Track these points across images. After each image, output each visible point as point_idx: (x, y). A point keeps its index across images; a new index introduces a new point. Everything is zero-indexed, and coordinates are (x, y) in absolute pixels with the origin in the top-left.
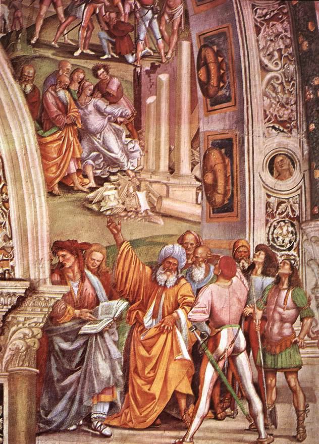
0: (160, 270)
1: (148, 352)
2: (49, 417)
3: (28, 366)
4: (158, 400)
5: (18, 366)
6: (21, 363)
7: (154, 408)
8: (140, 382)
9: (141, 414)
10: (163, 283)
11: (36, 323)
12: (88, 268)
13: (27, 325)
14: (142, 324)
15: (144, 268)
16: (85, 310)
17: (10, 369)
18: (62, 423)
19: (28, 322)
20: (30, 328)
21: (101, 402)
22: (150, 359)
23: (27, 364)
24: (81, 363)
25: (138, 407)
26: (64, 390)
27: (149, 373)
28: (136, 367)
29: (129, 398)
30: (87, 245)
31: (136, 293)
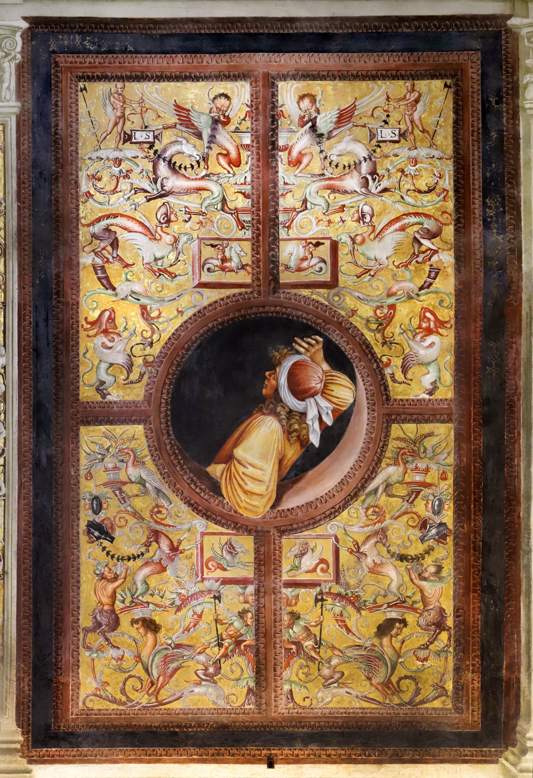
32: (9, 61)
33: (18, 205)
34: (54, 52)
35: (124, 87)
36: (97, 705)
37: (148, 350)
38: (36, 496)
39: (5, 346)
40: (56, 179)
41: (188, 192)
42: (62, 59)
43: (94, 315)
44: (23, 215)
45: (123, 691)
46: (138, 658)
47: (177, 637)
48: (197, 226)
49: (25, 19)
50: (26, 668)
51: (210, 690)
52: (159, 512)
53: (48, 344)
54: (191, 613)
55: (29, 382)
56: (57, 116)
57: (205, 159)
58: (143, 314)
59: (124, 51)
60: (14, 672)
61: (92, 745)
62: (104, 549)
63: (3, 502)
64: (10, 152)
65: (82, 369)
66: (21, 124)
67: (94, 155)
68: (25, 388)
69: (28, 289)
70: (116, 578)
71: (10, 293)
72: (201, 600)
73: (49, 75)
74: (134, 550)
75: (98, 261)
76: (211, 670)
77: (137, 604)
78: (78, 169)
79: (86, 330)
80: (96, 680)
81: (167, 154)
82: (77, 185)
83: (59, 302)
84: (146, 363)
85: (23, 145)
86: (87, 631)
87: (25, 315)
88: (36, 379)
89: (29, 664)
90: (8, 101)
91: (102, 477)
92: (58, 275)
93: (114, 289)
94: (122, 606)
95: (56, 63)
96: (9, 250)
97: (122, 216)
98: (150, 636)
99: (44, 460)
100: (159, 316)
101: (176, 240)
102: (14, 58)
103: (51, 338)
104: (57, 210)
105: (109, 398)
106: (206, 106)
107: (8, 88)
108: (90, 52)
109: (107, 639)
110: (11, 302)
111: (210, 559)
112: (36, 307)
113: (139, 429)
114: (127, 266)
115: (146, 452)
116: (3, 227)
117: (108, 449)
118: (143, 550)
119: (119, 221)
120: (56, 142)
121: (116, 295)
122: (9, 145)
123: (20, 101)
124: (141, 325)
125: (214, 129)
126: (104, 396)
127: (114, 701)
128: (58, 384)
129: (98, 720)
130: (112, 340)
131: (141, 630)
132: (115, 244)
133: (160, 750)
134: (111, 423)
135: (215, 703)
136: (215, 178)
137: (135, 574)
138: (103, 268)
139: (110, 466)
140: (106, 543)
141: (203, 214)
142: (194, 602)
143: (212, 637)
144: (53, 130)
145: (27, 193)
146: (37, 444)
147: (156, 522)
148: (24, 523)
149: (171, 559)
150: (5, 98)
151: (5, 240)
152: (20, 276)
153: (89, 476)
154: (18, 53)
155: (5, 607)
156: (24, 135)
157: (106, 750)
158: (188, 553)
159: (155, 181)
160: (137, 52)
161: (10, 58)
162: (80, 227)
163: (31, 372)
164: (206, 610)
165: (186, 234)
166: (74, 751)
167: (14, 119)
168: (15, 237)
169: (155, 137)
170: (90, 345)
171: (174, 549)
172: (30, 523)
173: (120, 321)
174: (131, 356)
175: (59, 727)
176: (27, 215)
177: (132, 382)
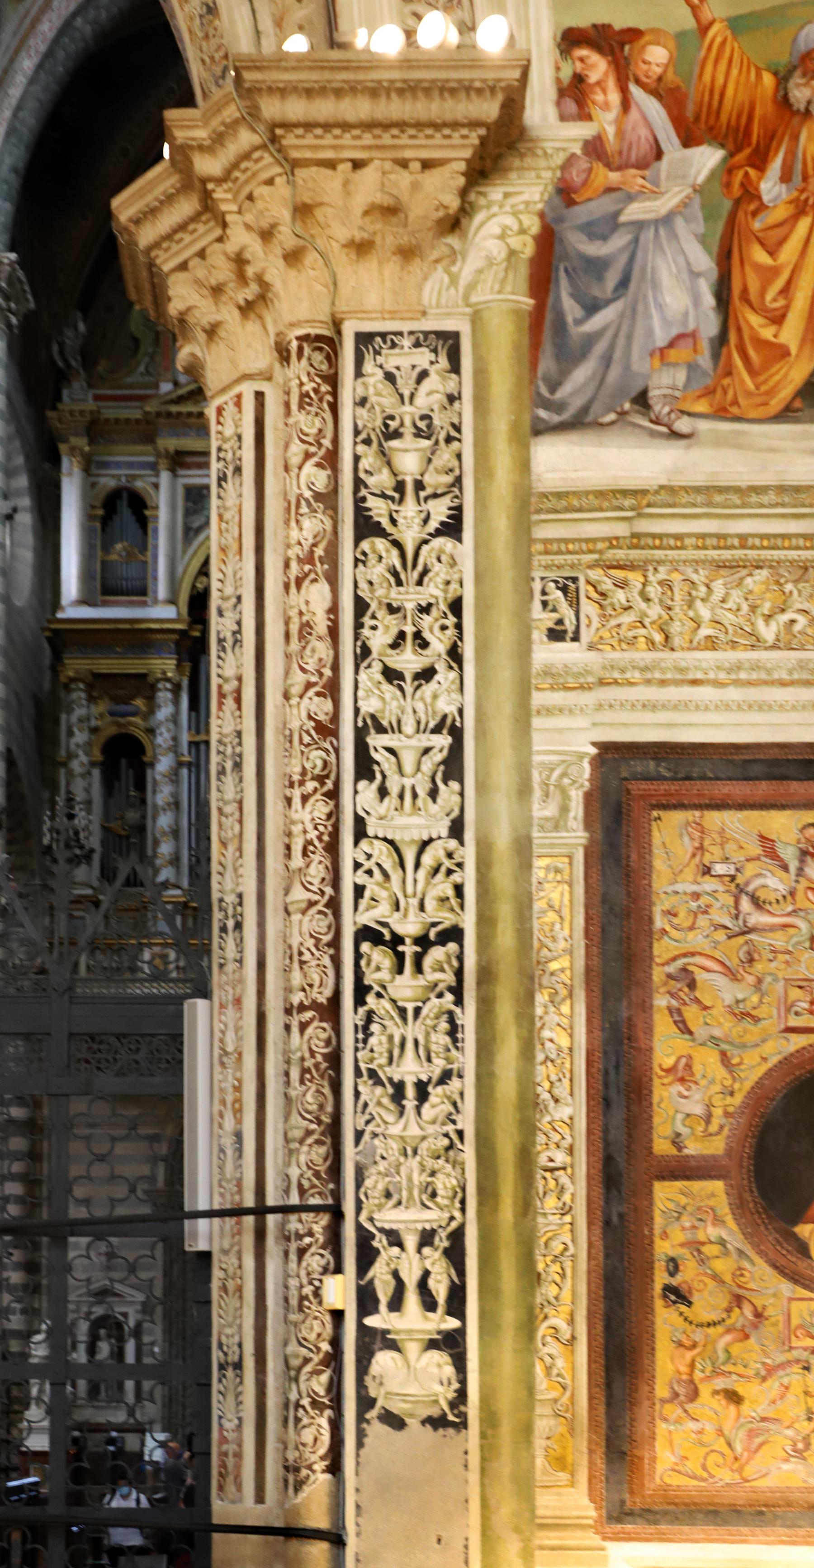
0: (797, 79)
1: (772, 254)
2: (559, 395)
3: (513, 293)
4: (797, 356)
5: (492, 293)
6: (497, 287)
7: (786, 374)
8: (755, 320)
9: (757, 388)
10: (802, 107)
11: (527, 203)
12: (638, 82)
13: (508, 208)
14: (759, 198)
15: (759, 76)
16: (632, 171)
17: (474, 299)
18: (585, 409)
19: (512, 201)
20: (515, 214)
21: (669, 364)
22: (775, 271)
23: (509, 288)
24: (624, 283)
25: (752, 372)
26: (590, 340)
27: (775, 300)
28: (745, 290)
29: (729, 356)
30: (634, 34)
31: (742, 130)
34: (626, 779)
35: (701, 817)
36: (675, 1480)
37: (729, 1100)
38: (607, 1256)
40: (628, 915)
41: (772, 928)
42: (636, 787)
43: (669, 1062)
45: (704, 1468)
46: (720, 1432)
47: (762, 1409)
48: (783, 966)
49: (594, 744)
51: (800, 1467)
52: (742, 1275)
54: (777, 1384)
55: (598, 1133)
57: (792, 893)
58: (722, 1061)
59: (703, 778)
61: (671, 1523)
62: (681, 1314)
65: (656, 1120)
67: (670, 889)
69: (597, 1033)
70: (694, 1346)
71: (576, 1038)
72: (788, 1370)
73: (619, 805)
74: (713, 1317)
75: (674, 1003)
76: (800, 1446)
77: (718, 1374)
78: (651, 904)
79: (660, 1077)
80: (673, 1453)
81: (750, 888)
82: (651, 921)
84: (727, 1114)
86: (663, 1401)
88: (606, 1131)
91: (678, 1236)
92: (629, 1019)
93: (691, 1033)
94: (701, 1375)
95: (628, 791)
97: (700, 954)
98: (732, 1408)
100: (739, 1064)
101: (760, 981)
102: (582, 786)
105: (686, 1151)
106: (793, 835)
107: (575, 818)
108: (665, 779)
109: (686, 1411)
111: (800, 1326)
112: (605, 1053)
113: (718, 1186)
114: (706, 1008)
115: (727, 1210)
117: (684, 1208)
118: (724, 1315)
119: (698, 960)
120: (628, 875)
121: (693, 1040)
124: (721, 1072)
125: (802, 861)
126: (680, 1149)
127: (694, 1477)
128: (630, 1135)
129: (676, 1497)
130: (688, 1089)
131: (724, 1402)
132: (692, 985)
133: (745, 1530)
134: (687, 1178)
135: (805, 1481)
136: (801, 914)
137: (715, 1341)
138: (679, 1012)
139: (687, 1224)
140: (683, 1308)
141: (789, 953)
142: (781, 1373)
143: (801, 1411)
145: (595, 930)
146: (607, 1201)
147: (739, 1286)
149: (755, 1326)
153: (665, 1235)
157: (686, 1528)
158: (773, 1319)
159: (737, 917)
160: (718, 779)
162: (654, 966)
164: (794, 1382)
165: (770, 974)
166: (652, 1529)
169: (737, 870)
170: (665, 1094)
171: (758, 1315)
173: (697, 1068)
174: (709, 1106)
177: (711, 1135)
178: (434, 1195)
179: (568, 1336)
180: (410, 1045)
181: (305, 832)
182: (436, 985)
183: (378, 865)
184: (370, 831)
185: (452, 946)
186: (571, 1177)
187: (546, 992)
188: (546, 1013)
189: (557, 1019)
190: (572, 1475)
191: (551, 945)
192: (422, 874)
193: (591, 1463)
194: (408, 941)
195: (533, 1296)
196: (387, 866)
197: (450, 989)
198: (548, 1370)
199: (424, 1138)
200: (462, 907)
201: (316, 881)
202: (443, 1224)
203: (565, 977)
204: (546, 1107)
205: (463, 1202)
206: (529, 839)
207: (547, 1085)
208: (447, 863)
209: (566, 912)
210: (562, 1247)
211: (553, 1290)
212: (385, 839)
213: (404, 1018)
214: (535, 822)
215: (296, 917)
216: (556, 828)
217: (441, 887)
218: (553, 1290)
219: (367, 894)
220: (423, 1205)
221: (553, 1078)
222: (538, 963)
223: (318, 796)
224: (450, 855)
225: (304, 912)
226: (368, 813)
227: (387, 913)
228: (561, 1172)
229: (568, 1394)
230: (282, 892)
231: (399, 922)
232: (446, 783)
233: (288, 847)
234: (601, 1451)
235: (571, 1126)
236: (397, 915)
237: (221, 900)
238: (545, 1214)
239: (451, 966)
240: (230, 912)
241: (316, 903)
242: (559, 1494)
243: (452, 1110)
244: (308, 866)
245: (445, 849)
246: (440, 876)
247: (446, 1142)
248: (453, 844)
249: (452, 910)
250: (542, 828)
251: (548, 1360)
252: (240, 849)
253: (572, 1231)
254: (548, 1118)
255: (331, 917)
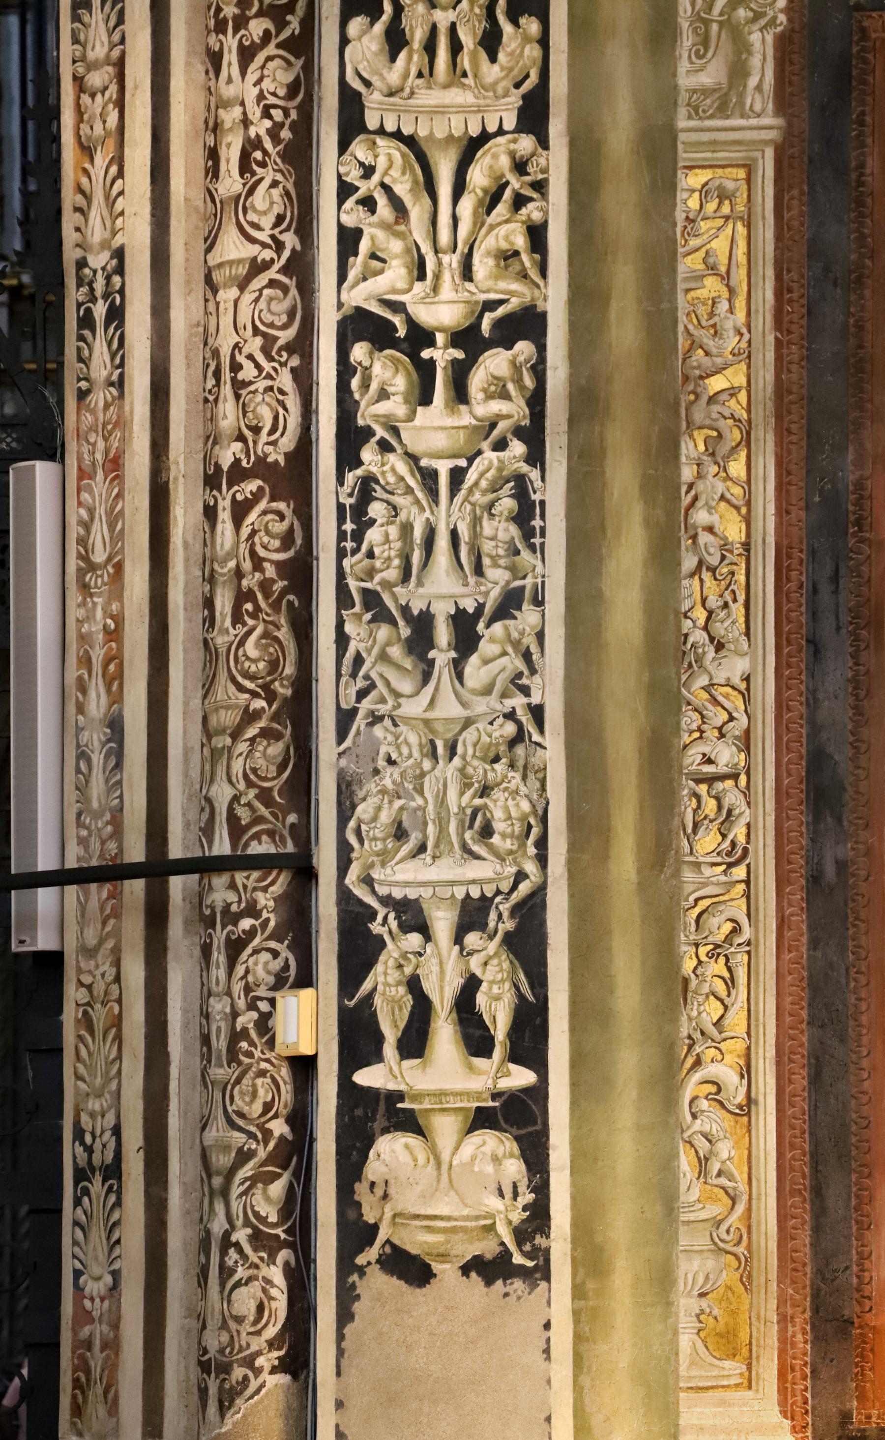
32: (761, 30)
33: (776, 338)
38: (814, 943)
39: (747, 634)
40: (859, 280)
44: (786, 359)
50: (797, 1297)
53: (838, 628)
55: (799, 708)
56: (863, 145)
60: (773, 1304)
63: (746, 957)
64: (761, 224)
66: (786, 162)
68: (789, 721)
69: (798, 514)
83: (862, 541)
85: (789, 209)
87: (789, 569)
88: (813, 702)
89: (804, 1288)
90: (759, 116)
92: (860, 485)
95: (863, 31)
96: (758, 433)
99: (830, 870)
102: (773, 22)
103: (845, 618)
104: (861, 347)
107: (759, 88)
110: (760, 541)
112: (813, 552)
116: (745, 384)
120: (860, 203)
122: (759, 209)
123: (784, 115)
128: (858, 711)
144: (854, 176)
145: (796, 311)
148: (789, 999)
150: (751, 109)
151: (749, 411)
152: (779, 488)
154: (781, 11)
155: (753, 1171)
156: (791, 187)
161: (763, 22)
163: (803, 688)
167: (770, 153)
168: (770, 405)
172: (802, 999)
175: (869, 1417)
176: (796, 358)
178: (487, 831)
179: (741, 1098)
180: (442, 543)
181: (246, 122)
182: (493, 425)
183: (384, 186)
184: (372, 122)
185: (524, 348)
186: (747, 793)
187: (700, 437)
188: (700, 476)
189: (720, 487)
190: (749, 1367)
191: (710, 343)
192: (467, 206)
193: (783, 1340)
194: (440, 338)
195: (675, 1021)
196: (401, 189)
197: (519, 432)
198: (703, 1163)
199: (468, 723)
200: (543, 272)
201: (267, 222)
202: (505, 887)
203: (737, 406)
204: (699, 660)
205: (542, 843)
206: (671, 133)
207: (700, 615)
208: (515, 183)
209: (740, 276)
210: (728, 927)
211: (714, 1009)
212: (398, 135)
213: (433, 493)
214: (683, 97)
215: (228, 295)
216: (722, 110)
217: (503, 230)
218: (714, 1009)
219: (364, 246)
220: (466, 849)
221: (713, 602)
222: (686, 378)
223: (271, 49)
224: (520, 167)
225: (242, 287)
226: (367, 84)
227: (402, 285)
228: (729, 783)
229: (740, 1208)
230: (203, 247)
231: (422, 301)
232: (516, 24)
233: (213, 154)
234: (802, 1318)
235: (746, 696)
236: (419, 288)
237: (82, 264)
238: (697, 865)
239: (522, 387)
240: (99, 286)
241: (267, 265)
242: (723, 1403)
243: (521, 666)
244: (251, 192)
245: (512, 154)
246: (502, 209)
247: (510, 729)
248: (526, 144)
249: (524, 276)
250: (695, 111)
251: (702, 1145)
252: (119, 160)
253: (747, 895)
254: (704, 681)
255: (294, 292)
